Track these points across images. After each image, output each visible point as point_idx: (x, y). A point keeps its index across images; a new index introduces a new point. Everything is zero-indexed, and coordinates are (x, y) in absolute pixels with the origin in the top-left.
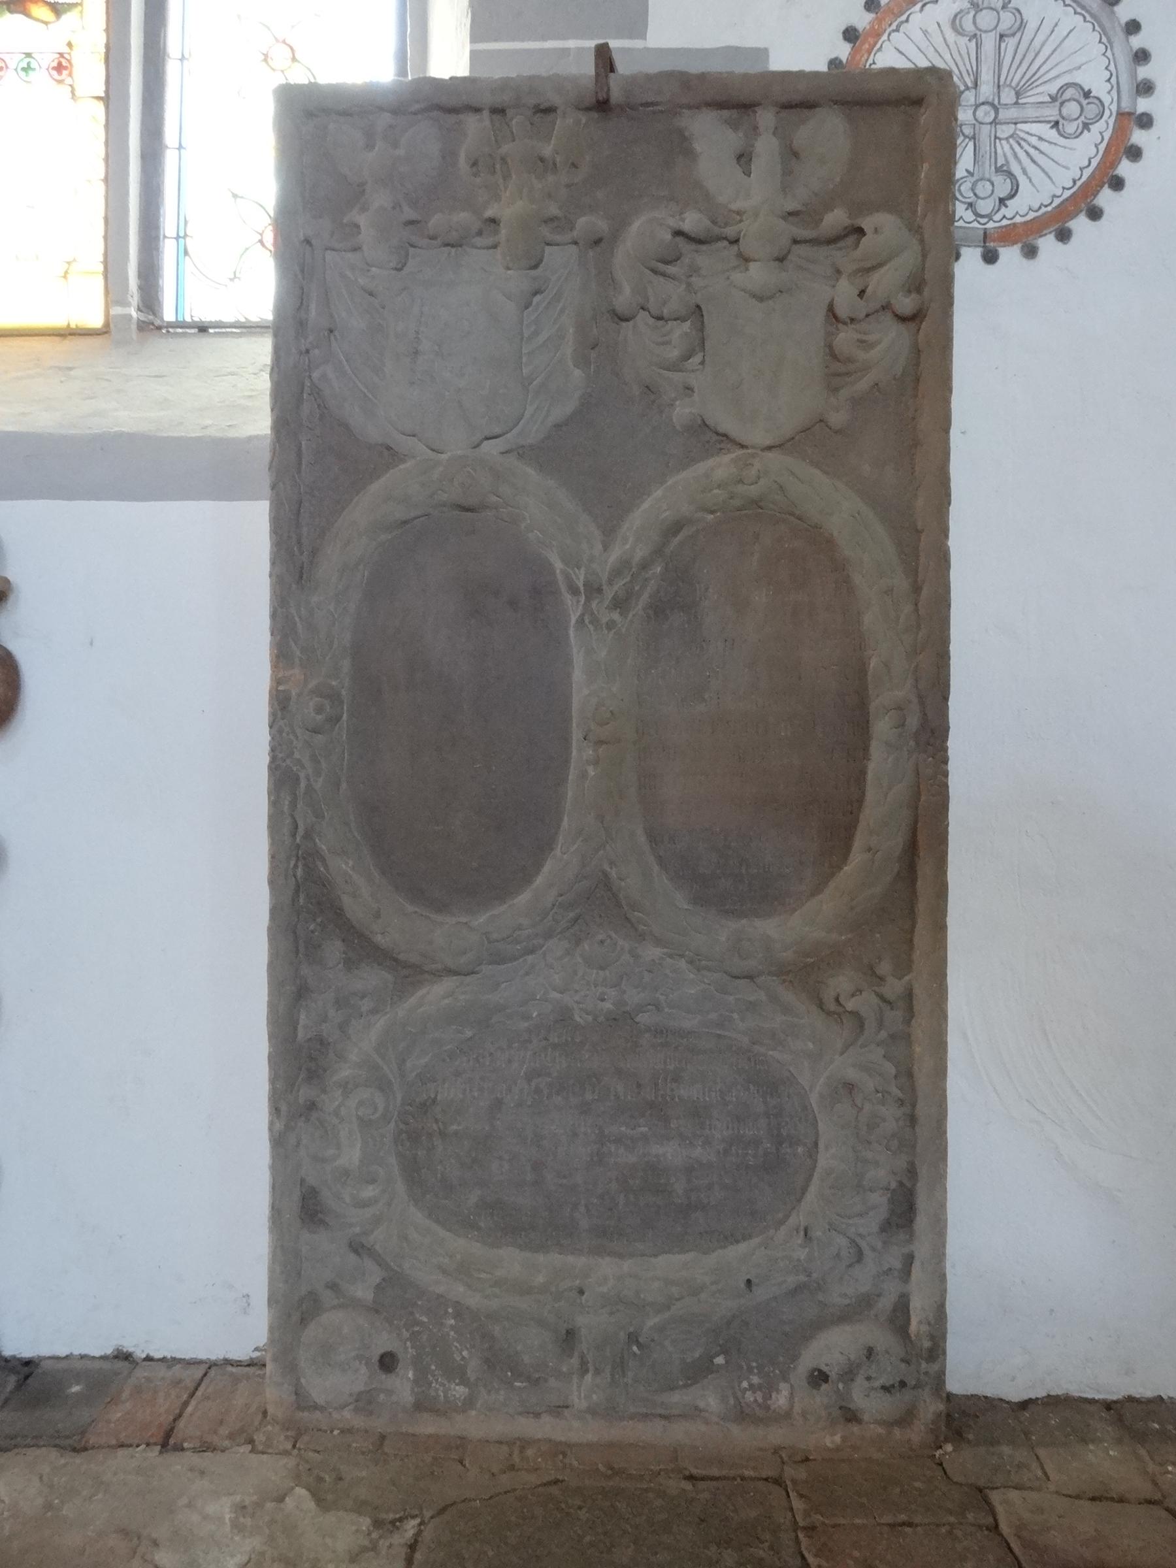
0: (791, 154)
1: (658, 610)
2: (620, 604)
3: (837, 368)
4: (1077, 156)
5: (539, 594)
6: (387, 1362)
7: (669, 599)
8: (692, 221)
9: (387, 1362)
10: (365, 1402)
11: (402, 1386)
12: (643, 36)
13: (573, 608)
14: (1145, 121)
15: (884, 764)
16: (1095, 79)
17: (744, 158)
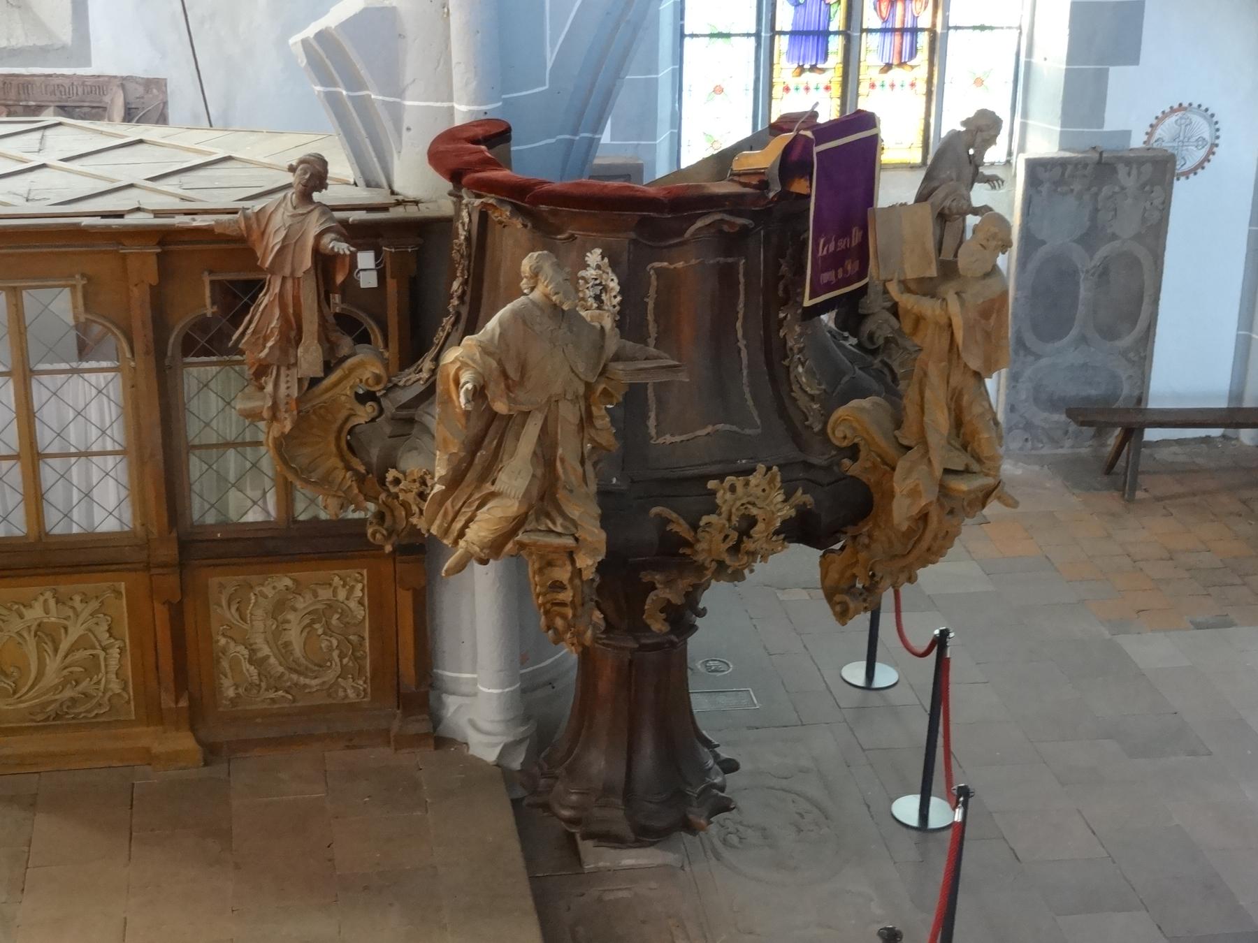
0: (1139, 173)
1: (1100, 276)
2: (1093, 275)
3: (1144, 220)
4: (1202, 153)
5: (1076, 272)
6: (1027, 440)
7: (1103, 273)
8: (1117, 189)
9: (1027, 440)
10: (1021, 449)
11: (1029, 444)
12: (1102, 126)
13: (1082, 276)
14: (1217, 145)
15: (1146, 308)
16: (1207, 135)
17: (1129, 174)
